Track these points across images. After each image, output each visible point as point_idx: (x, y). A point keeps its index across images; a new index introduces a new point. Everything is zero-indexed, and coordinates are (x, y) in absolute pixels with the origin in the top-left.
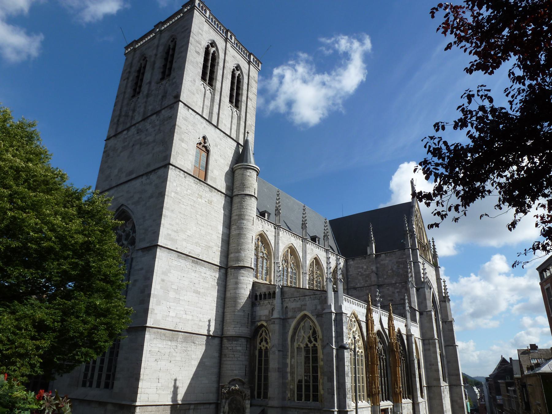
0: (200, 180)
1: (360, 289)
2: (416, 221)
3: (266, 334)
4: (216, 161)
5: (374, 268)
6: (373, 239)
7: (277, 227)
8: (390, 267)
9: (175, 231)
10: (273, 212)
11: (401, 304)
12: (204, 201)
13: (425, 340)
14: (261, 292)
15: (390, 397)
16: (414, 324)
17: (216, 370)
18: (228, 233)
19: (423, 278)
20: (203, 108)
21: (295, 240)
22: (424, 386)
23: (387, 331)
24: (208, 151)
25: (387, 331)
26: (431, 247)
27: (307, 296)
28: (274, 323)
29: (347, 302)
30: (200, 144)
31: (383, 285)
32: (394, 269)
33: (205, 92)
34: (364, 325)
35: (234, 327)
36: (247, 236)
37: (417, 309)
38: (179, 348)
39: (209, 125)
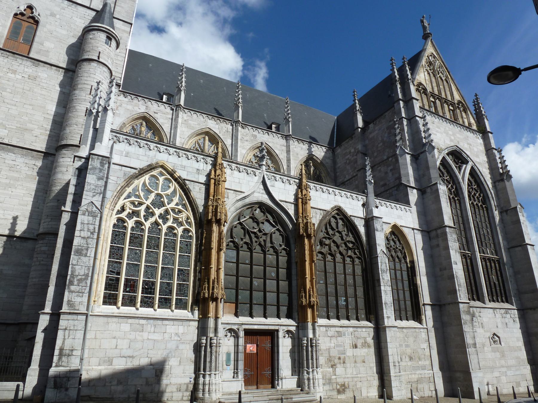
1: (348, 182)
5: (360, 147)
6: (358, 108)
8: (380, 139)
12: (20, 77)
13: (430, 231)
21: (217, 124)
22: (424, 305)
24: (37, 22)
30: (22, 14)
32: (385, 139)
36: (78, 107)
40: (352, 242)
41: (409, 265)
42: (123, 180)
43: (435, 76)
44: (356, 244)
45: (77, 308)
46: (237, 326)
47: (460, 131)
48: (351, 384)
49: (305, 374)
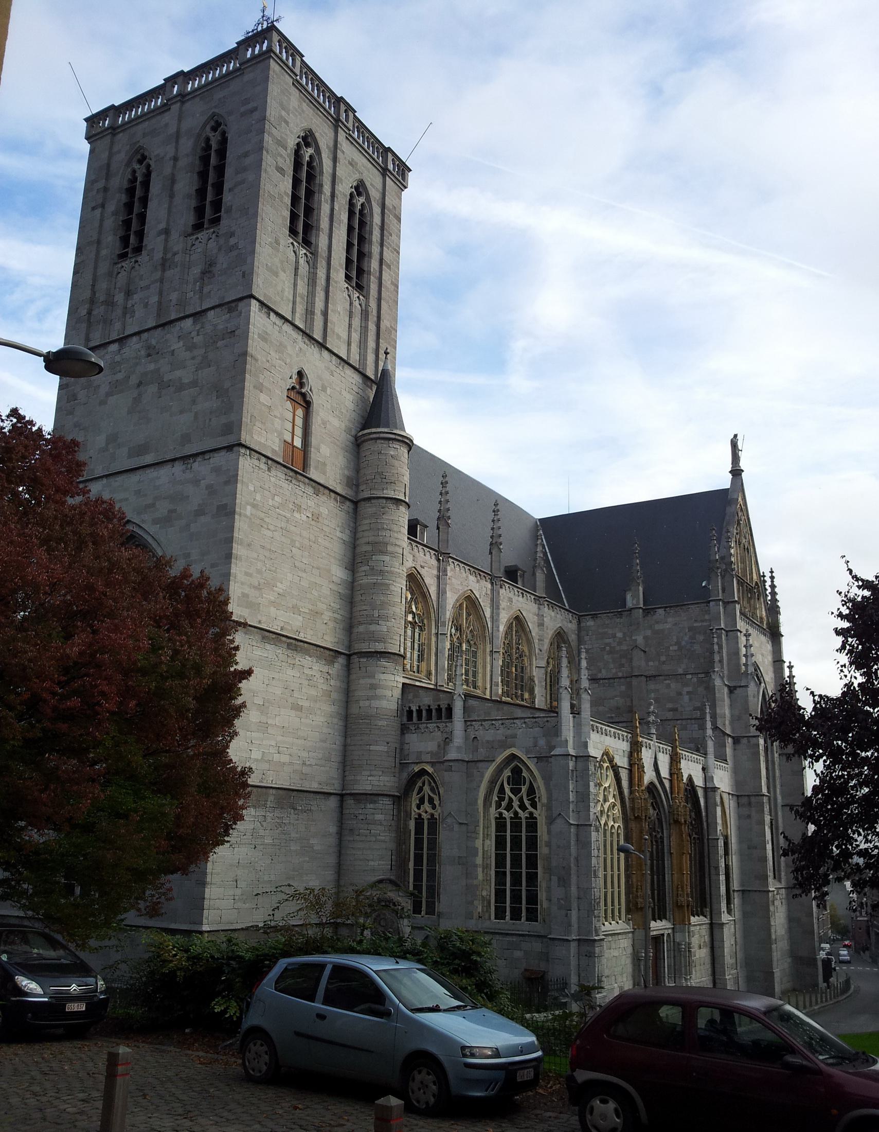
0: (296, 472)
1: (606, 681)
2: (737, 534)
3: (432, 790)
4: (324, 423)
7: (442, 555)
9: (255, 587)
10: (433, 524)
11: (695, 719)
12: (304, 518)
14: (421, 705)
16: (721, 764)
17: (332, 860)
18: (350, 580)
19: (744, 665)
20: (294, 303)
21: (478, 581)
22: (734, 891)
26: (766, 590)
27: (517, 718)
28: (450, 769)
29: (595, 732)
31: (659, 676)
32: (683, 643)
33: (297, 262)
34: (624, 775)
35: (368, 776)
36: (392, 588)
37: (728, 732)
38: (269, 820)
39: (309, 343)
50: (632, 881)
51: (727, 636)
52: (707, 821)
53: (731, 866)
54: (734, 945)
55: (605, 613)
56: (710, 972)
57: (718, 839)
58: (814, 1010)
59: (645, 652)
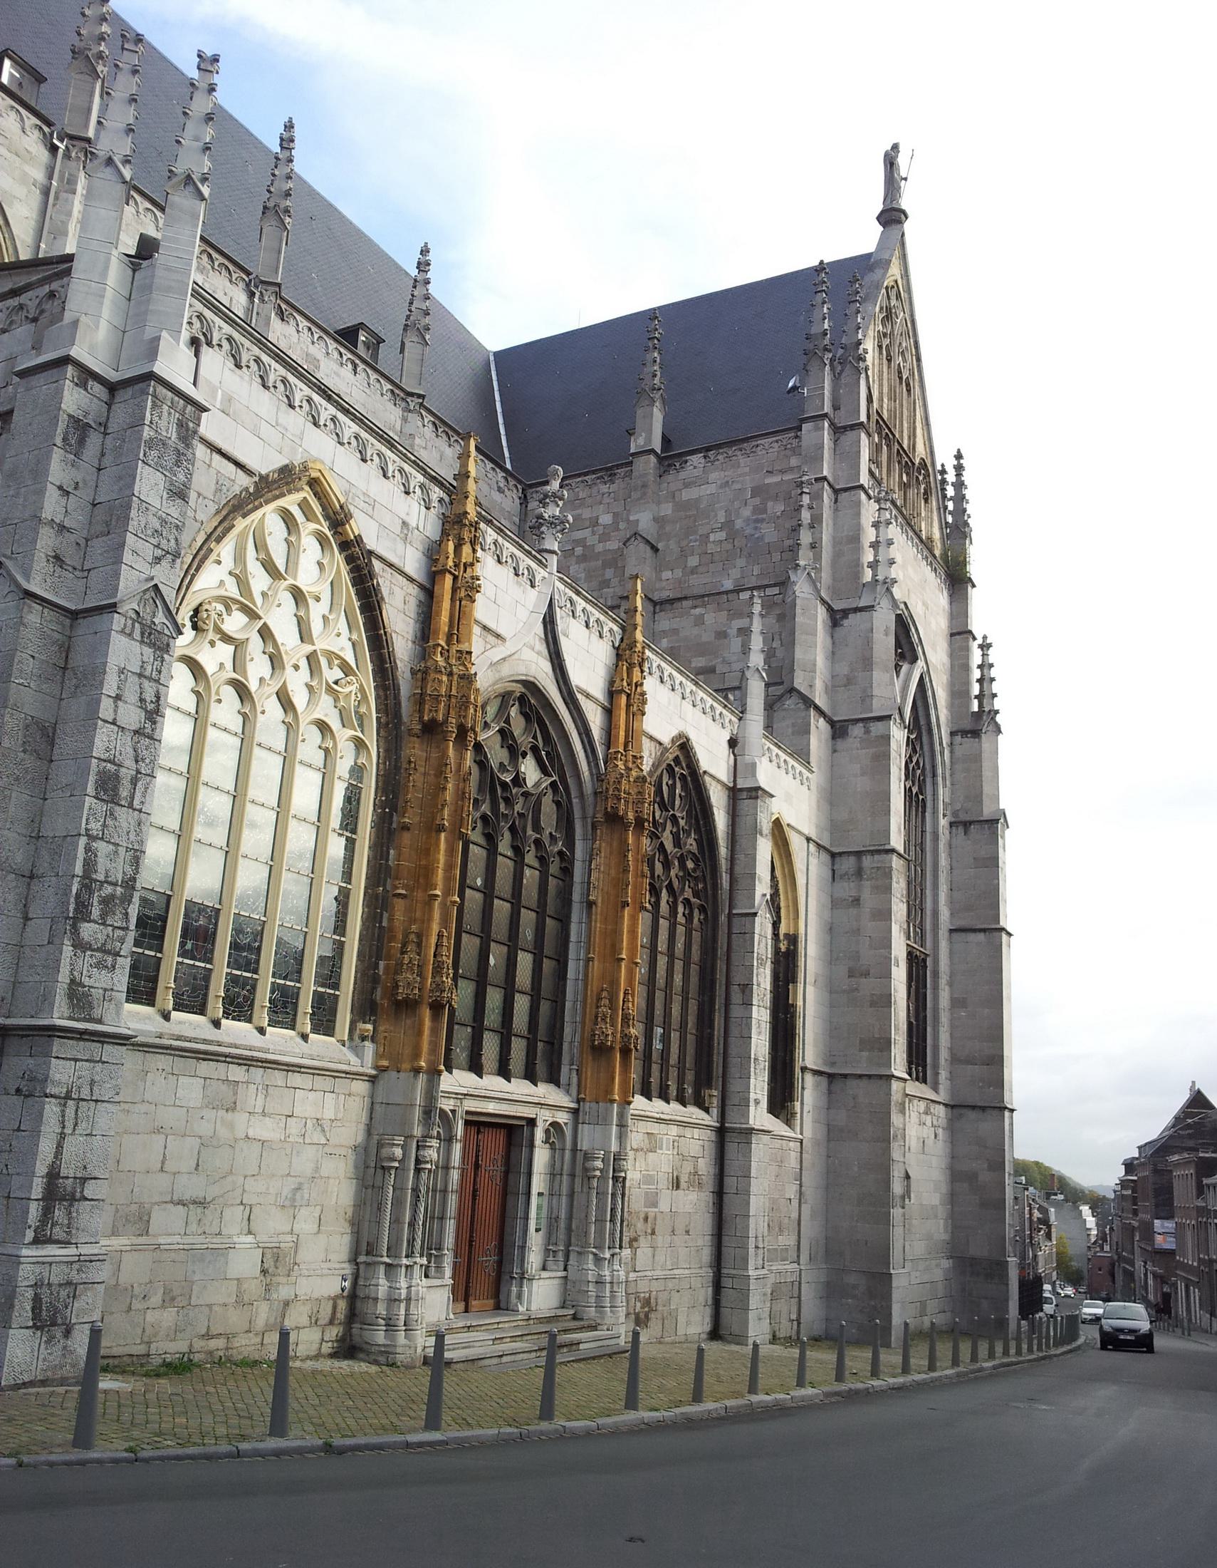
15: (565, 1069)
19: (870, 565)
22: (804, 1069)
23: (595, 719)
25: (595, 719)
32: (739, 524)
37: (820, 700)
40: (696, 860)
41: (783, 947)
42: (213, 508)
43: (889, 361)
44: (702, 864)
45: (96, 1013)
46: (452, 1102)
47: (916, 558)
48: (663, 1297)
49: (591, 1266)
50: (391, 920)
51: (836, 501)
52: (731, 871)
53: (800, 1009)
54: (795, 1203)
55: (579, 475)
56: (706, 1255)
57: (755, 914)
58: (981, 1370)
59: (655, 549)
